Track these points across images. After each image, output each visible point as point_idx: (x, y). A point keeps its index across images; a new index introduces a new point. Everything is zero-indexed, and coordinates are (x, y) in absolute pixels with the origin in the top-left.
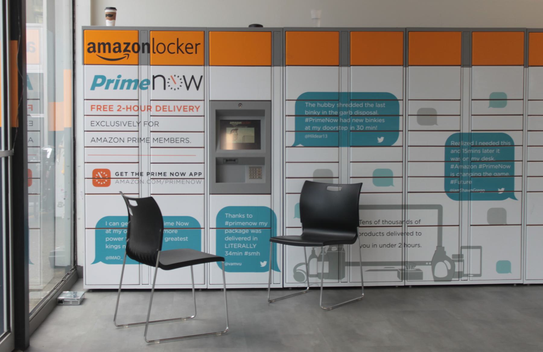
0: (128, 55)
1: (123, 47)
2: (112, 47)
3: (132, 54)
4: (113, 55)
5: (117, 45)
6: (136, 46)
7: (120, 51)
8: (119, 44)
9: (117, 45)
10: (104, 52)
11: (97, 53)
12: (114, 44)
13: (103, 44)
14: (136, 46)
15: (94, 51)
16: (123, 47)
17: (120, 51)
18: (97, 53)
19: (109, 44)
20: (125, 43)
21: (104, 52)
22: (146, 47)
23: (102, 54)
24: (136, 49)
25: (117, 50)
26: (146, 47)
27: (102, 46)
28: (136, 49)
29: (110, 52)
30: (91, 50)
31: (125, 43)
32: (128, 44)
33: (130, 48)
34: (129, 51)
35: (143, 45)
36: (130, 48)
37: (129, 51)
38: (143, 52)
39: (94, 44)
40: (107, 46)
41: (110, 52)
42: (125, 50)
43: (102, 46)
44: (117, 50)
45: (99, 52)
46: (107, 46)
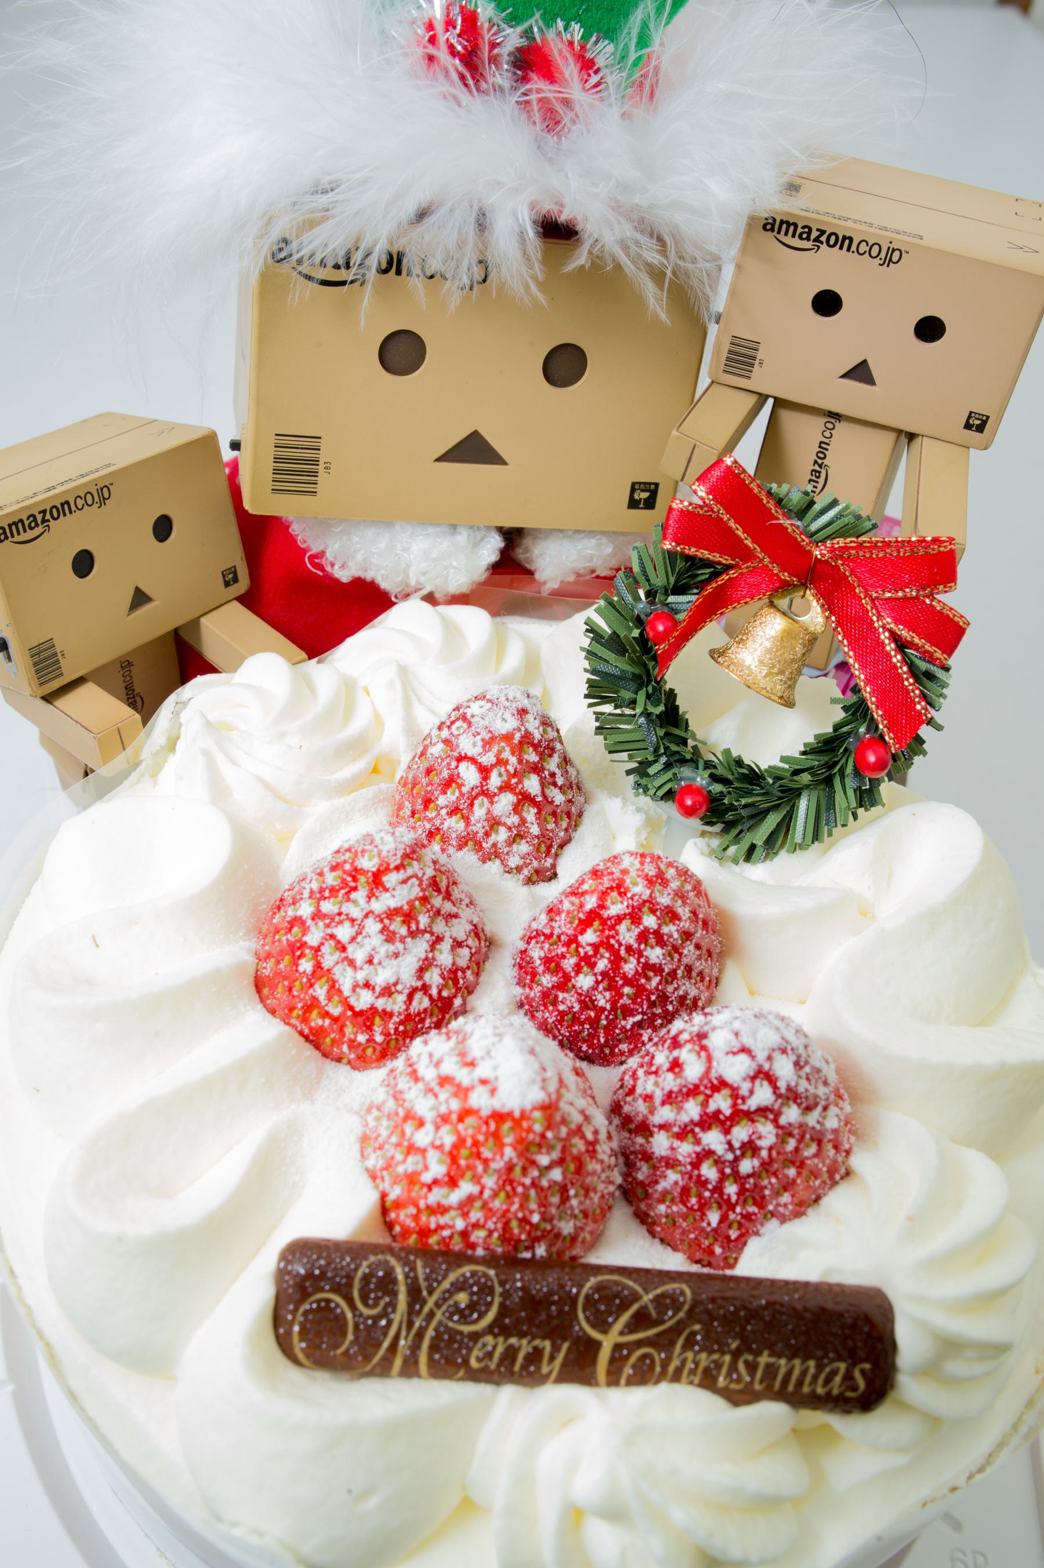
0: (819, 247)
1: (815, 234)
2: (799, 230)
3: (824, 247)
4: (796, 242)
5: (806, 230)
6: (833, 238)
7: (808, 239)
8: (810, 229)
9: (806, 230)
10: (786, 234)
11: (775, 233)
12: (803, 228)
14: (833, 238)
15: (772, 230)
16: (815, 234)
18: (775, 233)
19: (795, 225)
20: (818, 230)
21: (786, 234)
22: (847, 242)
23: (782, 237)
24: (832, 242)
25: (804, 236)
26: (847, 242)
27: (784, 226)
28: (832, 242)
29: (793, 236)
31: (818, 230)
32: (823, 232)
33: (823, 238)
34: (822, 243)
35: (844, 238)
36: (823, 238)
37: (822, 243)
38: (841, 248)
39: (774, 220)
40: (792, 228)
42: (817, 240)
43: (784, 226)
44: (804, 236)
45: (779, 232)
46: (792, 228)
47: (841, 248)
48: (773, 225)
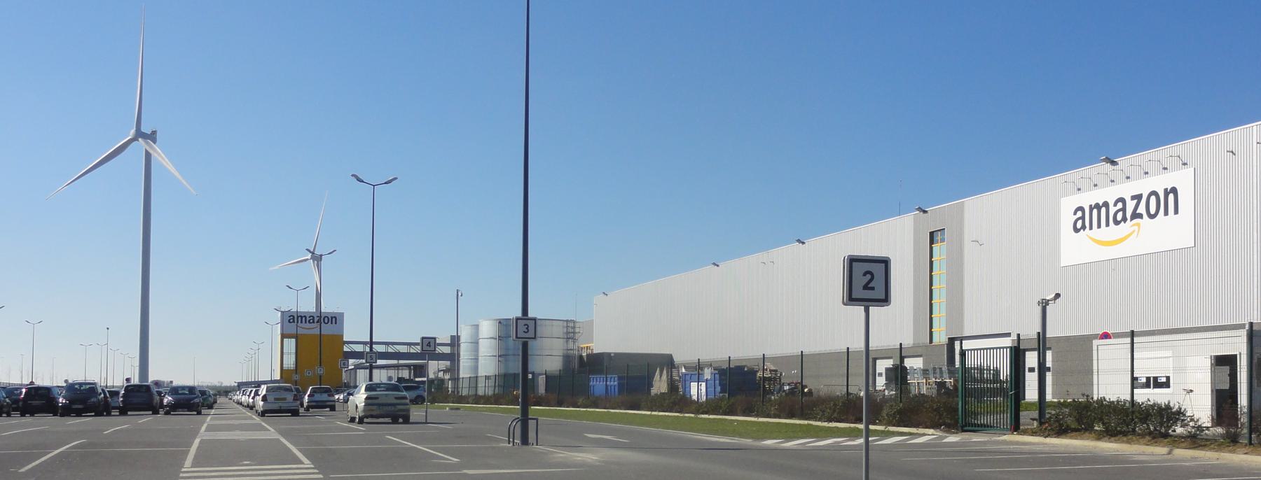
2: (308, 319)
4: (308, 325)
7: (314, 322)
10: (301, 322)
12: (310, 317)
13: (301, 316)
15: (294, 322)
17: (314, 322)
21: (301, 322)
22: (334, 319)
24: (326, 318)
25: (311, 321)
26: (334, 319)
27: (300, 318)
28: (326, 318)
29: (306, 322)
30: (291, 321)
35: (332, 318)
38: (332, 323)
40: (304, 318)
41: (306, 322)
43: (300, 318)
44: (311, 321)
46: (304, 318)
47: (332, 323)
48: (294, 319)
